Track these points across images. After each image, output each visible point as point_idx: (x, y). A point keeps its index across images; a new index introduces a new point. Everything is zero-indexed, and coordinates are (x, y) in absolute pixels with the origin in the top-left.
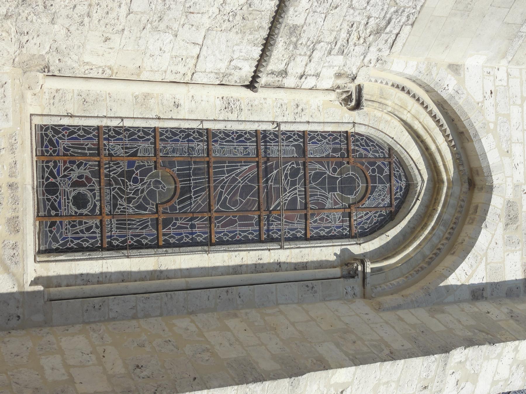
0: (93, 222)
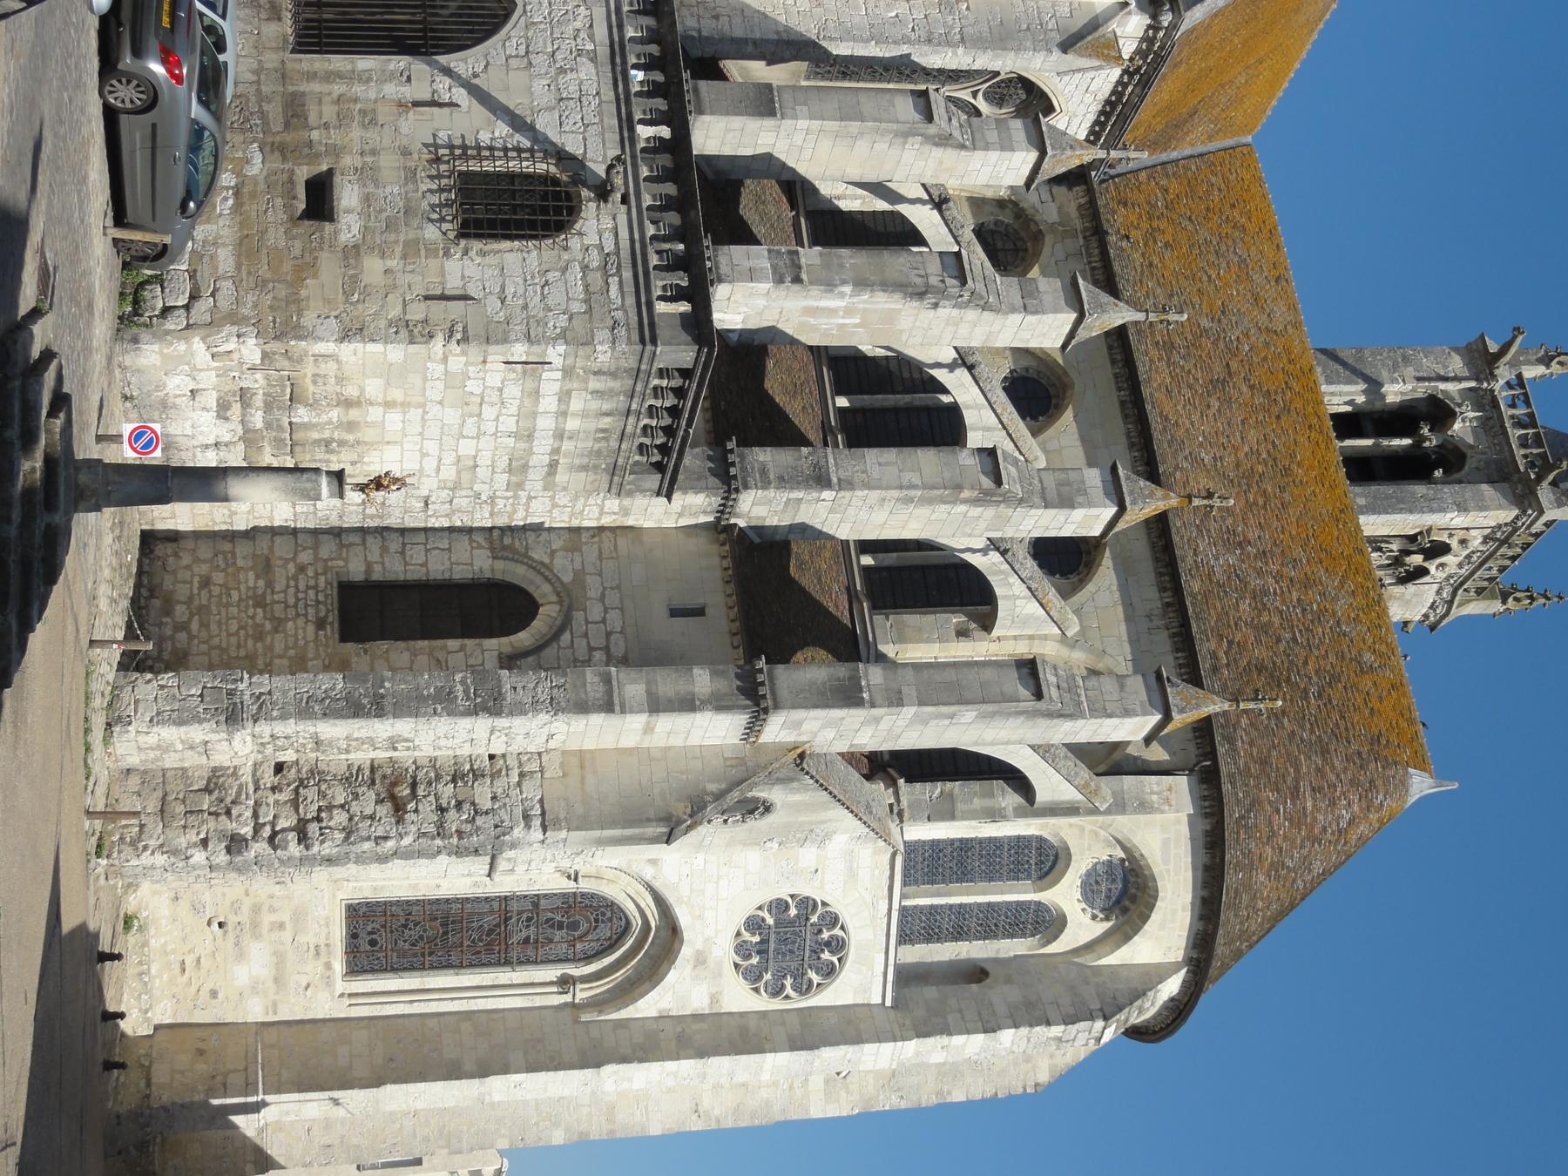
0: (381, 955)
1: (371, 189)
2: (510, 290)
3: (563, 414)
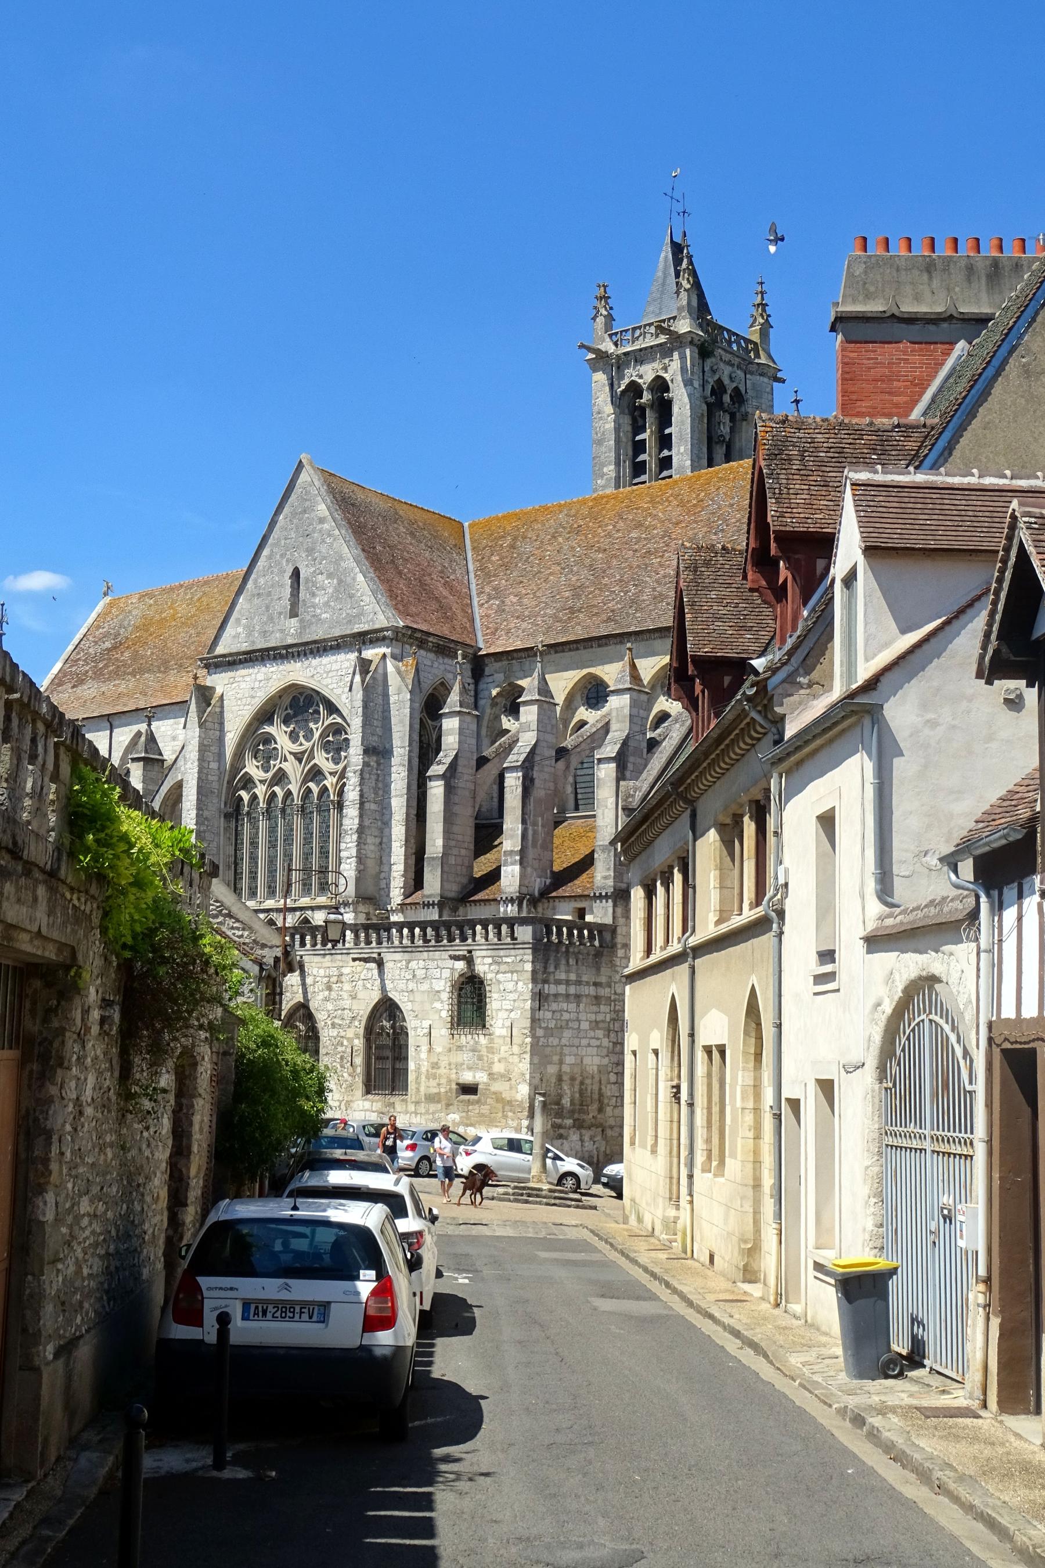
1: (465, 1066)
3: (568, 982)
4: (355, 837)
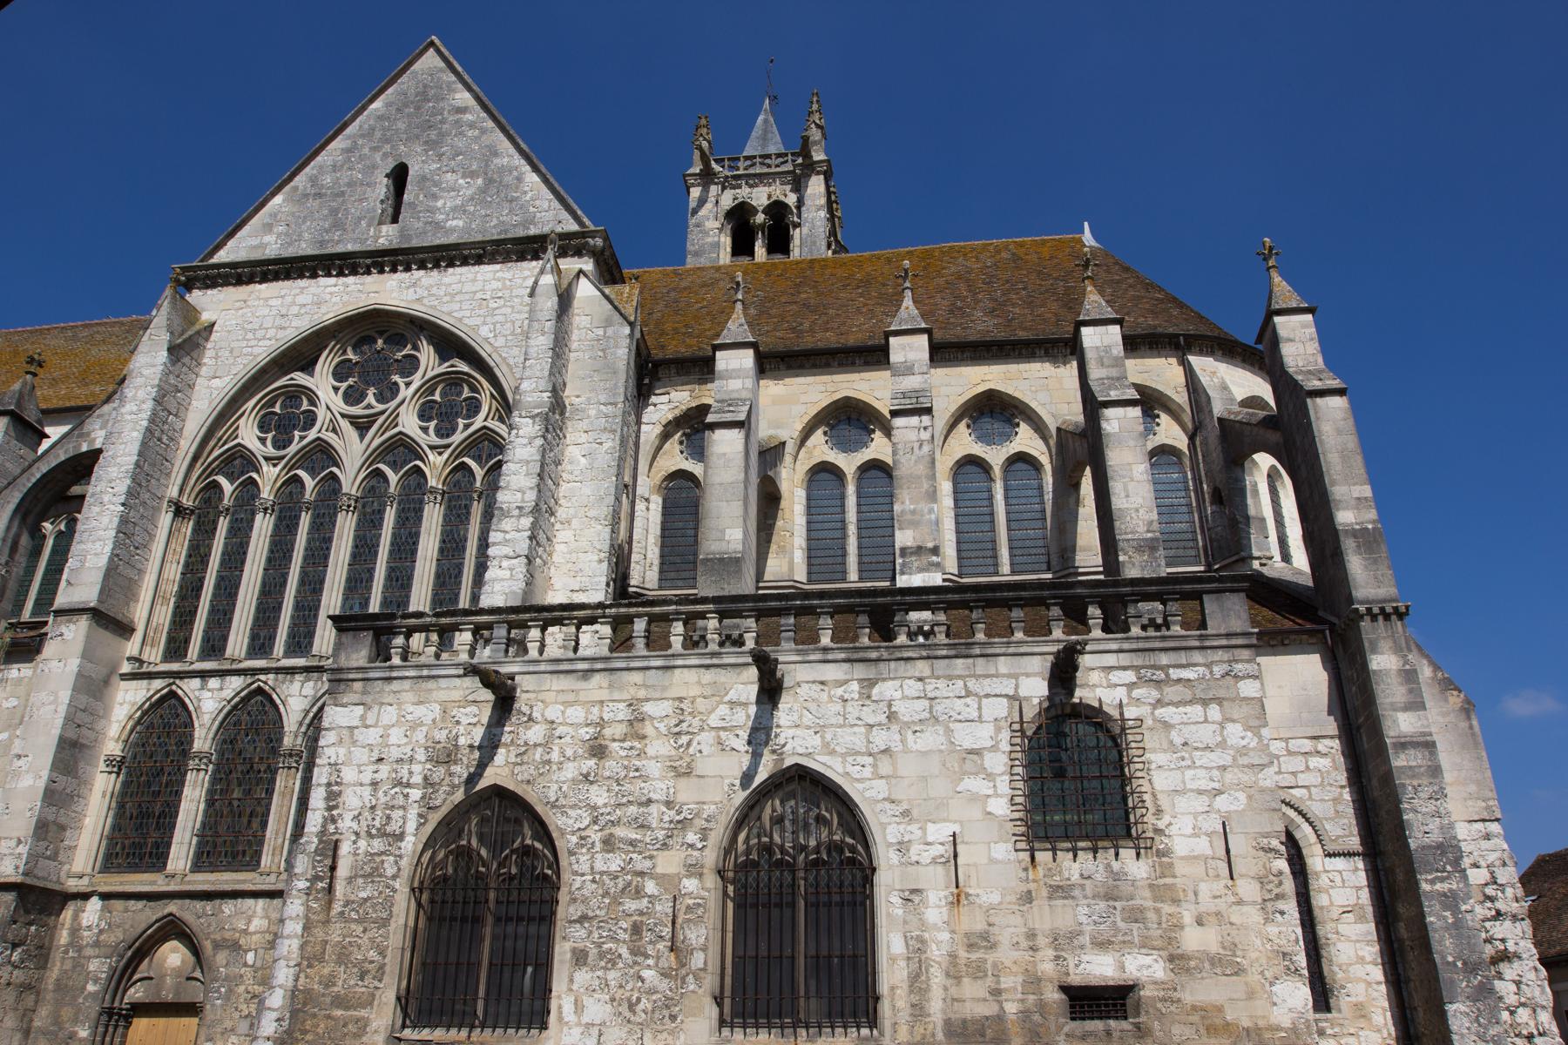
1: (1085, 940)
2: (1204, 784)
4: (526, 522)
